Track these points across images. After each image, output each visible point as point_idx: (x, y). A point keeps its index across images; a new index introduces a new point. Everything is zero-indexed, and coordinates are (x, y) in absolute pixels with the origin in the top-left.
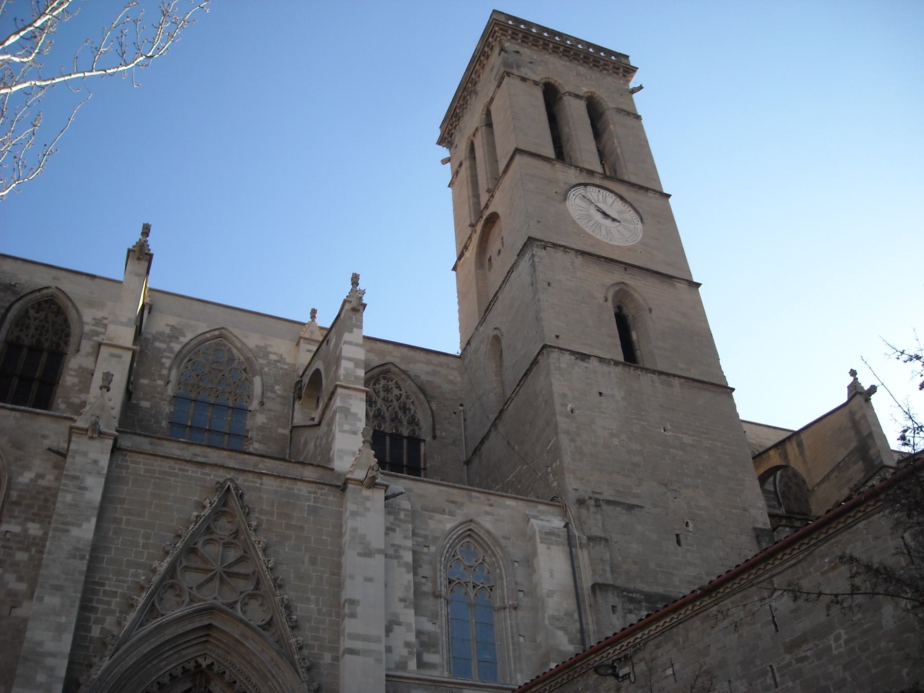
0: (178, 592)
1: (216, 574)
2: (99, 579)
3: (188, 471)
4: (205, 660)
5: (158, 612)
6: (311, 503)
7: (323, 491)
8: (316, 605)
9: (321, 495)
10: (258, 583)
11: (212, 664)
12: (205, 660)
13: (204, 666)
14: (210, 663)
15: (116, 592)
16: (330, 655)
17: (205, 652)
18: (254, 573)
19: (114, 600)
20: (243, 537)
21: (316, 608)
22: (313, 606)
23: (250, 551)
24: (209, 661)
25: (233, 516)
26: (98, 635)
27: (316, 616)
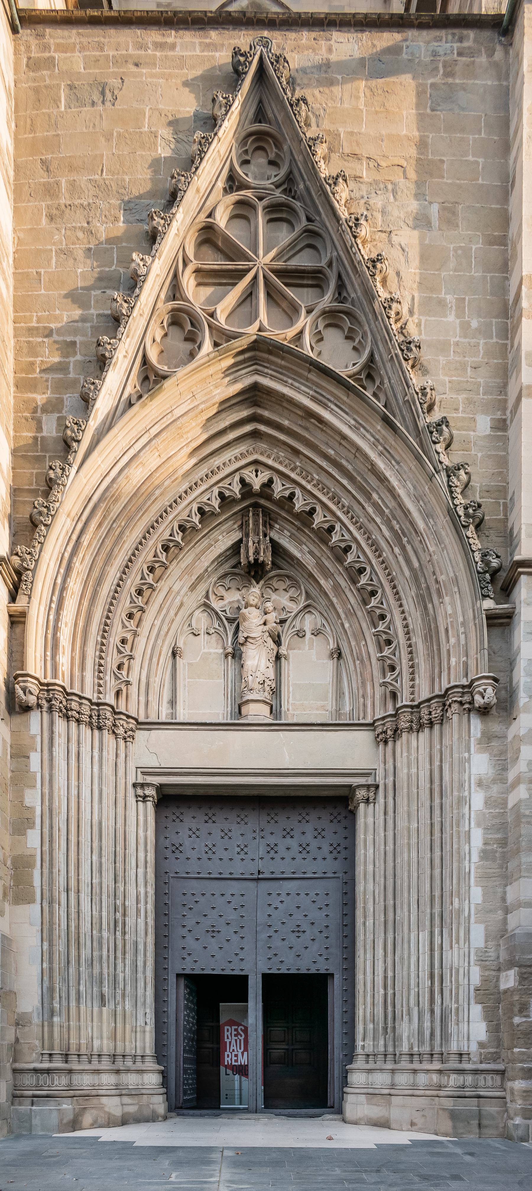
0: (189, 327)
1: (255, 277)
2: (38, 322)
3: (173, 47)
4: (257, 476)
5: (157, 375)
6: (438, 79)
7: (466, 44)
8: (457, 316)
9: (460, 54)
10: (341, 286)
11: (271, 481)
12: (257, 476)
13: (257, 487)
14: (266, 480)
15: (74, 343)
16: (489, 418)
17: (255, 457)
18: (330, 265)
19: (72, 359)
20: (301, 186)
21: (458, 321)
22: (451, 318)
23: (319, 214)
24: (264, 476)
25: (278, 145)
26: (54, 434)
27: (457, 339)
